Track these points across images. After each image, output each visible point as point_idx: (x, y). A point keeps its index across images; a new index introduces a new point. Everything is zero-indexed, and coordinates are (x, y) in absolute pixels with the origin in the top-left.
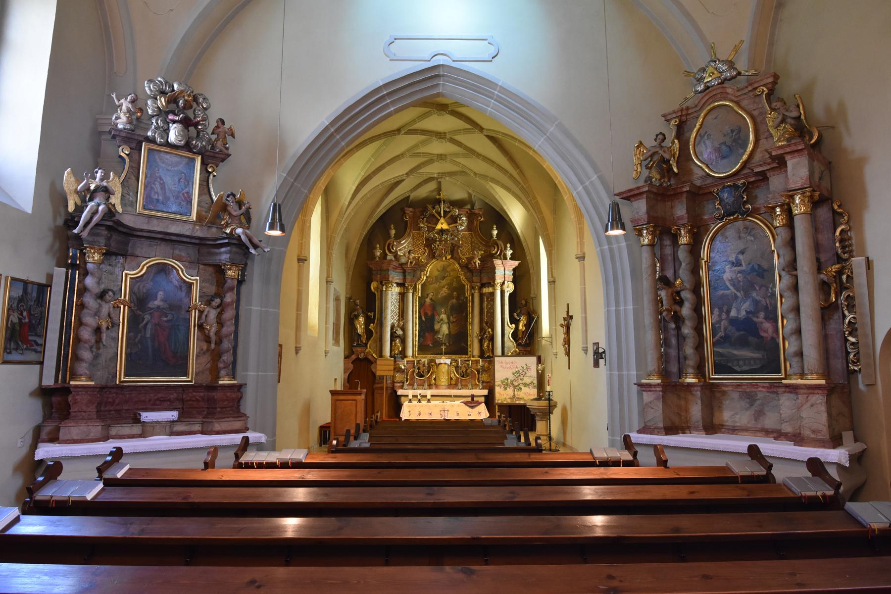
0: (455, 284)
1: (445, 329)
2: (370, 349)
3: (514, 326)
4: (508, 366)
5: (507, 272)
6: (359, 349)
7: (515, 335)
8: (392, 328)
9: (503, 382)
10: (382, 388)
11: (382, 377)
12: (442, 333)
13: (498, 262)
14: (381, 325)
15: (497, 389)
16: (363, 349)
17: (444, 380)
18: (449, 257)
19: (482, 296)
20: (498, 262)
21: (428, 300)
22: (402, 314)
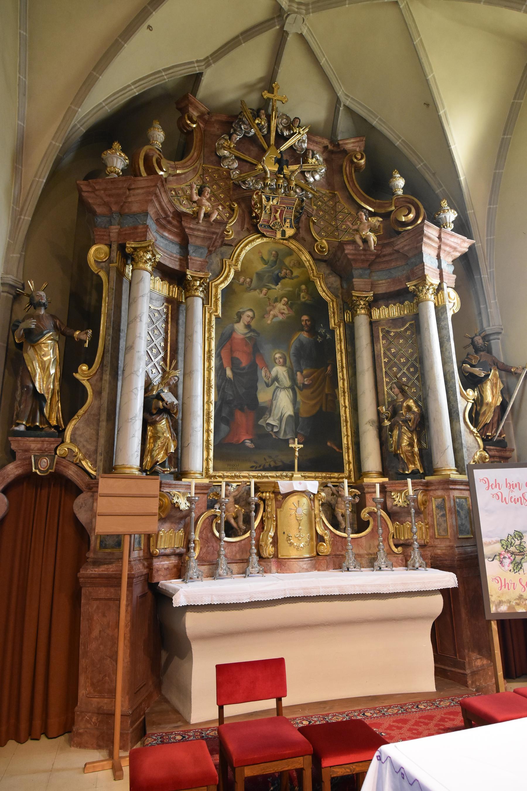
0: (304, 297)
1: (284, 404)
2: (75, 444)
3: (471, 394)
4: (517, 494)
5: (444, 265)
6: (34, 444)
7: (475, 417)
8: (148, 385)
9: (506, 544)
10: (114, 581)
11: (117, 541)
12: (276, 413)
13: (431, 231)
14: (114, 370)
15: (493, 570)
16: (48, 443)
17: (298, 544)
18: (290, 232)
19: (372, 324)
20: (431, 231)
21: (240, 328)
22: (174, 351)
